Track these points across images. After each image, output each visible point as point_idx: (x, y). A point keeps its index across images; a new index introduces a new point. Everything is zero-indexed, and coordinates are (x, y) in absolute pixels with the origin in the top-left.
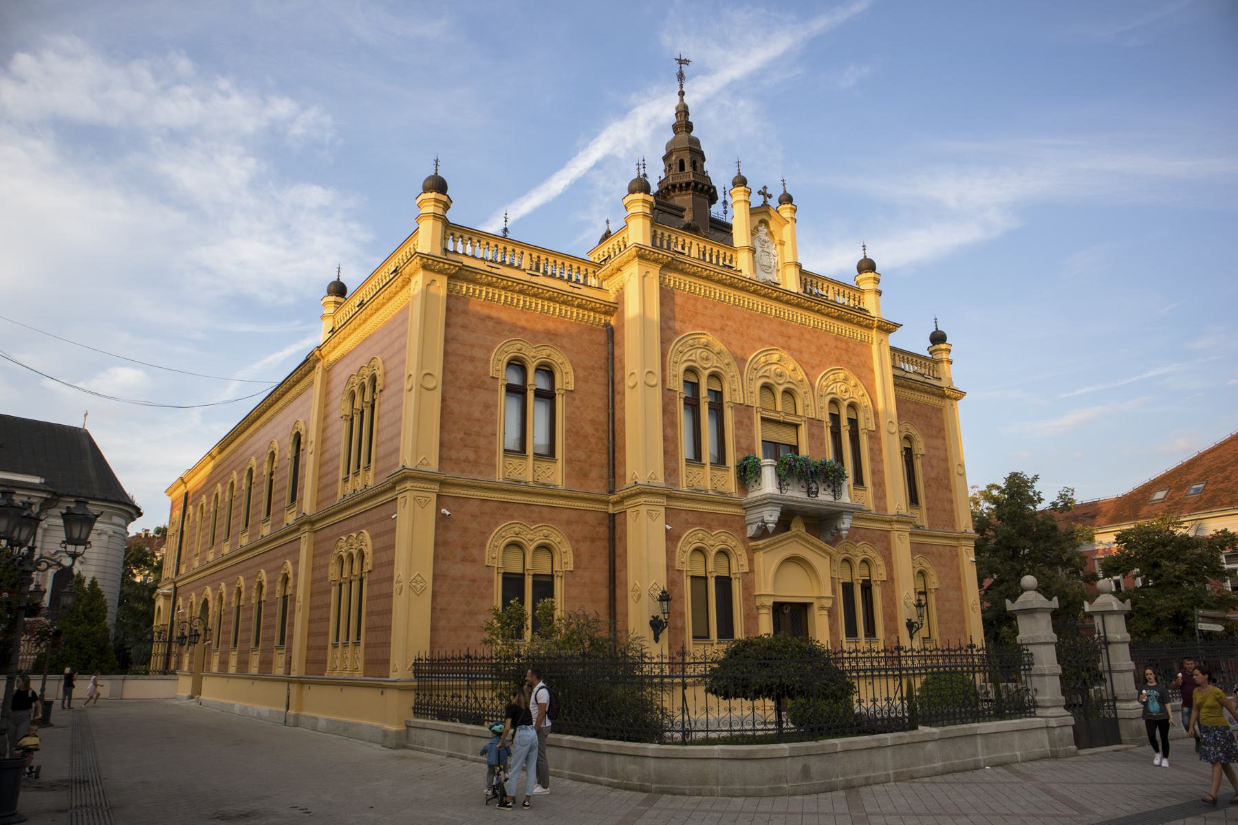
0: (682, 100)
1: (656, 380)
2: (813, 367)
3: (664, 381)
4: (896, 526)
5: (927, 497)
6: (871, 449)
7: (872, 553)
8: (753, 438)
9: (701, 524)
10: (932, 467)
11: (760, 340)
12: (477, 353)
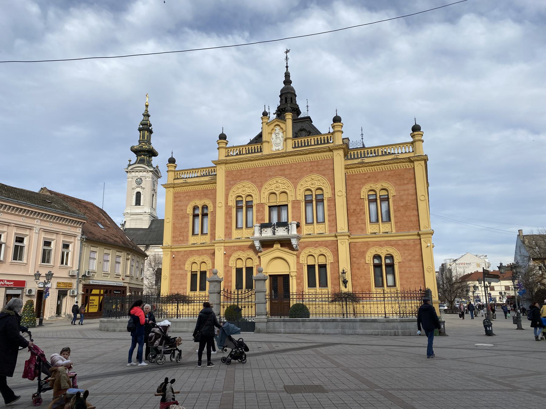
0: (287, 70)
2: (296, 179)
3: (227, 203)
5: (395, 217)
6: (328, 206)
7: (324, 250)
9: (240, 250)
12: (184, 208)
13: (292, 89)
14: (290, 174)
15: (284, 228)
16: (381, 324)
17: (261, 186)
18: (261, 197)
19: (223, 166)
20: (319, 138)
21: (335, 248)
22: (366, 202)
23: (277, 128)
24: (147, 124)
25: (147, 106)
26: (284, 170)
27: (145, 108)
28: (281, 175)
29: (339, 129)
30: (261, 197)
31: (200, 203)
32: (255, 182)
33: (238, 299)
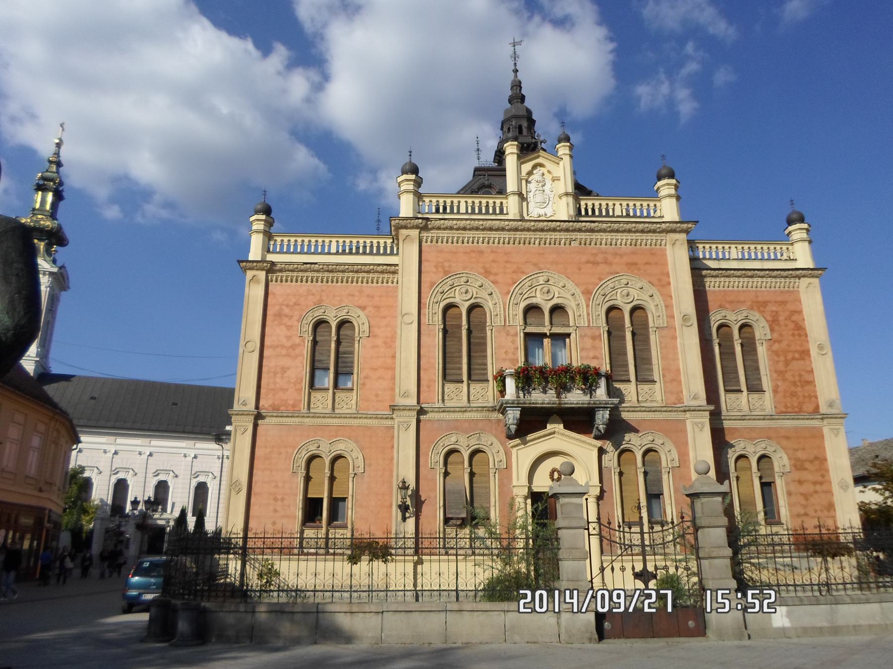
0: (516, 76)
4: (688, 414)
7: (659, 441)
23: (538, 172)
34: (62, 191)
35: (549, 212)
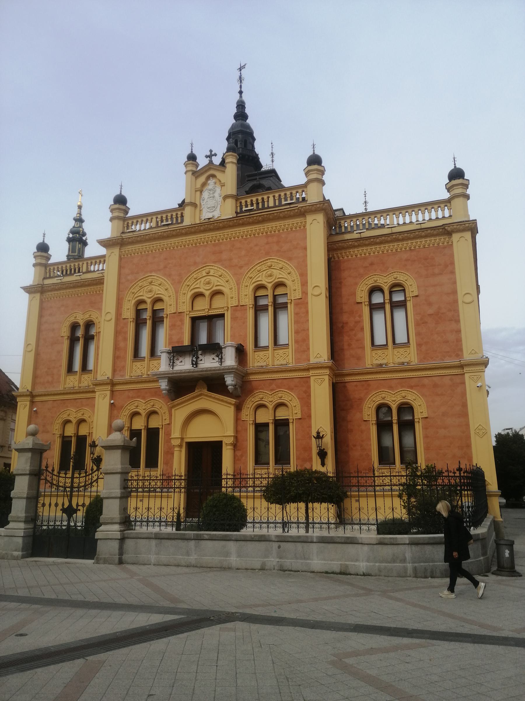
0: (241, 97)
1: (113, 315)
2: (241, 267)
4: (311, 372)
5: (418, 334)
8: (182, 333)
9: (138, 397)
10: (430, 304)
11: (195, 263)
13: (248, 127)
14: (230, 260)
15: (213, 356)
16: (366, 548)
17: (179, 282)
18: (177, 303)
19: (116, 251)
20: (282, 194)
21: (305, 392)
22: (366, 310)
23: (211, 182)
24: (78, 233)
25: (80, 207)
26: (221, 252)
27: (76, 210)
28: (215, 262)
29: (319, 177)
30: (177, 303)
31: (81, 319)
32: (169, 276)
33: (72, 487)
34: (86, 239)
35: (216, 214)
